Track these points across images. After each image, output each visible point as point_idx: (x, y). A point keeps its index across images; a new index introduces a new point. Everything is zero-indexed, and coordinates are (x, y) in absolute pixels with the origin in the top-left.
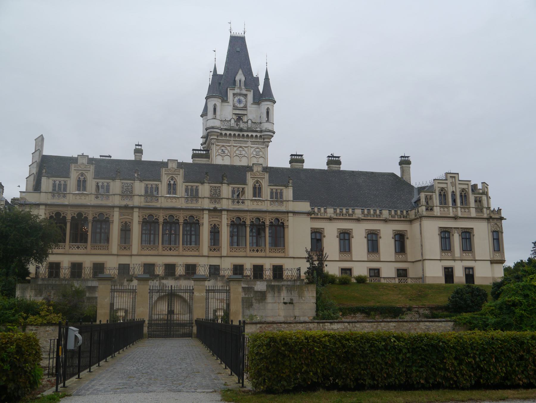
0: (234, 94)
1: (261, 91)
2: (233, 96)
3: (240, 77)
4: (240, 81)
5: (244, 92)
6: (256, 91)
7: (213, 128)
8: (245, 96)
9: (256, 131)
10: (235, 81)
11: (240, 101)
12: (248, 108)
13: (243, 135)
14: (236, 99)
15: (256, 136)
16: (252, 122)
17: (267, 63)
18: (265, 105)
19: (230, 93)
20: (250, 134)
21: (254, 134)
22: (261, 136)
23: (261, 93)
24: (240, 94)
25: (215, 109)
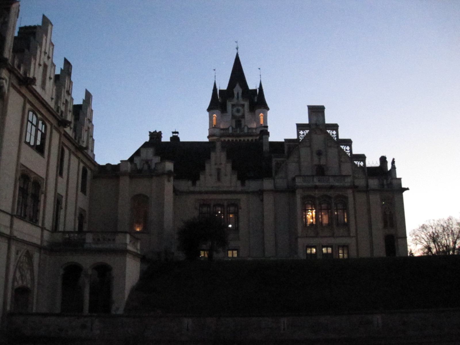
0: (233, 106)
2: (232, 107)
3: (238, 90)
4: (238, 94)
8: (243, 106)
9: (251, 136)
10: (233, 93)
11: (238, 111)
14: (235, 109)
17: (260, 75)
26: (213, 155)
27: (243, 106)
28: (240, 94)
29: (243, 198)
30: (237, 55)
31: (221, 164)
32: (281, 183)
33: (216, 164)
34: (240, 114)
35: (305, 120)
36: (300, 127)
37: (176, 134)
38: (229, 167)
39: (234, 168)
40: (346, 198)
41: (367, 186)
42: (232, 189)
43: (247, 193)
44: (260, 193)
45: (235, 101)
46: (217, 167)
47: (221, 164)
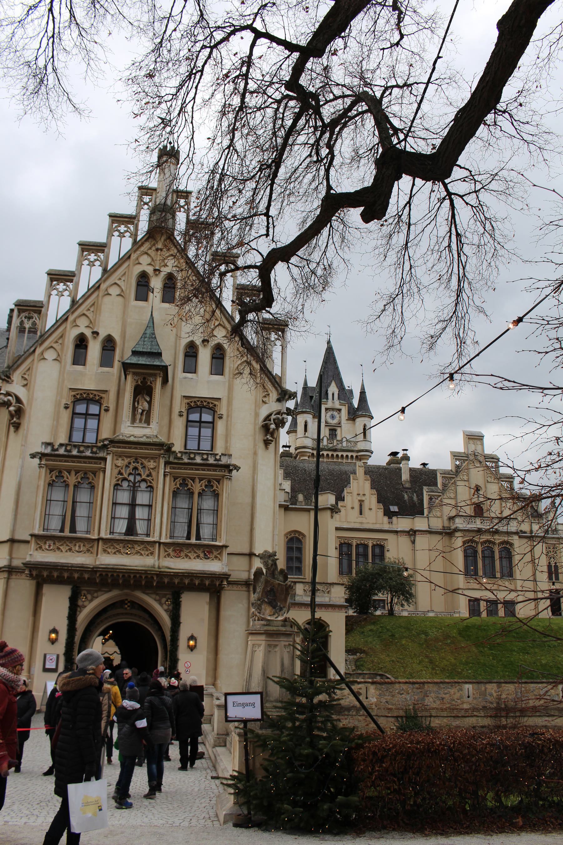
0: (327, 409)
1: (356, 406)
3: (333, 389)
4: (333, 394)
5: (337, 406)
6: (351, 405)
7: (304, 447)
8: (340, 410)
10: (327, 394)
12: (342, 424)
13: (337, 456)
14: (330, 413)
15: (352, 456)
16: (347, 440)
18: (360, 422)
19: (323, 407)
20: (345, 454)
21: (349, 454)
22: (357, 456)
23: (356, 407)
24: (333, 409)
25: (306, 426)
26: (353, 483)
27: (340, 410)
28: (336, 396)
29: (391, 538)
30: (329, 342)
31: (364, 495)
32: (437, 524)
33: (358, 494)
34: (335, 421)
35: (460, 448)
36: (455, 456)
37: (287, 449)
38: (374, 499)
39: (379, 502)
40: (511, 545)
41: (531, 532)
42: (377, 527)
43: (396, 532)
44: (412, 533)
45: (330, 404)
46: (359, 498)
47: (364, 495)
